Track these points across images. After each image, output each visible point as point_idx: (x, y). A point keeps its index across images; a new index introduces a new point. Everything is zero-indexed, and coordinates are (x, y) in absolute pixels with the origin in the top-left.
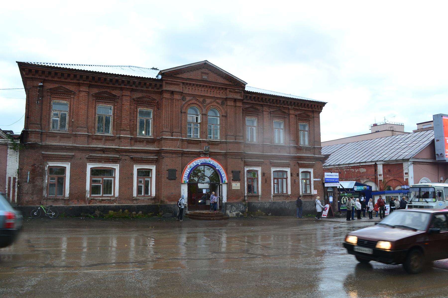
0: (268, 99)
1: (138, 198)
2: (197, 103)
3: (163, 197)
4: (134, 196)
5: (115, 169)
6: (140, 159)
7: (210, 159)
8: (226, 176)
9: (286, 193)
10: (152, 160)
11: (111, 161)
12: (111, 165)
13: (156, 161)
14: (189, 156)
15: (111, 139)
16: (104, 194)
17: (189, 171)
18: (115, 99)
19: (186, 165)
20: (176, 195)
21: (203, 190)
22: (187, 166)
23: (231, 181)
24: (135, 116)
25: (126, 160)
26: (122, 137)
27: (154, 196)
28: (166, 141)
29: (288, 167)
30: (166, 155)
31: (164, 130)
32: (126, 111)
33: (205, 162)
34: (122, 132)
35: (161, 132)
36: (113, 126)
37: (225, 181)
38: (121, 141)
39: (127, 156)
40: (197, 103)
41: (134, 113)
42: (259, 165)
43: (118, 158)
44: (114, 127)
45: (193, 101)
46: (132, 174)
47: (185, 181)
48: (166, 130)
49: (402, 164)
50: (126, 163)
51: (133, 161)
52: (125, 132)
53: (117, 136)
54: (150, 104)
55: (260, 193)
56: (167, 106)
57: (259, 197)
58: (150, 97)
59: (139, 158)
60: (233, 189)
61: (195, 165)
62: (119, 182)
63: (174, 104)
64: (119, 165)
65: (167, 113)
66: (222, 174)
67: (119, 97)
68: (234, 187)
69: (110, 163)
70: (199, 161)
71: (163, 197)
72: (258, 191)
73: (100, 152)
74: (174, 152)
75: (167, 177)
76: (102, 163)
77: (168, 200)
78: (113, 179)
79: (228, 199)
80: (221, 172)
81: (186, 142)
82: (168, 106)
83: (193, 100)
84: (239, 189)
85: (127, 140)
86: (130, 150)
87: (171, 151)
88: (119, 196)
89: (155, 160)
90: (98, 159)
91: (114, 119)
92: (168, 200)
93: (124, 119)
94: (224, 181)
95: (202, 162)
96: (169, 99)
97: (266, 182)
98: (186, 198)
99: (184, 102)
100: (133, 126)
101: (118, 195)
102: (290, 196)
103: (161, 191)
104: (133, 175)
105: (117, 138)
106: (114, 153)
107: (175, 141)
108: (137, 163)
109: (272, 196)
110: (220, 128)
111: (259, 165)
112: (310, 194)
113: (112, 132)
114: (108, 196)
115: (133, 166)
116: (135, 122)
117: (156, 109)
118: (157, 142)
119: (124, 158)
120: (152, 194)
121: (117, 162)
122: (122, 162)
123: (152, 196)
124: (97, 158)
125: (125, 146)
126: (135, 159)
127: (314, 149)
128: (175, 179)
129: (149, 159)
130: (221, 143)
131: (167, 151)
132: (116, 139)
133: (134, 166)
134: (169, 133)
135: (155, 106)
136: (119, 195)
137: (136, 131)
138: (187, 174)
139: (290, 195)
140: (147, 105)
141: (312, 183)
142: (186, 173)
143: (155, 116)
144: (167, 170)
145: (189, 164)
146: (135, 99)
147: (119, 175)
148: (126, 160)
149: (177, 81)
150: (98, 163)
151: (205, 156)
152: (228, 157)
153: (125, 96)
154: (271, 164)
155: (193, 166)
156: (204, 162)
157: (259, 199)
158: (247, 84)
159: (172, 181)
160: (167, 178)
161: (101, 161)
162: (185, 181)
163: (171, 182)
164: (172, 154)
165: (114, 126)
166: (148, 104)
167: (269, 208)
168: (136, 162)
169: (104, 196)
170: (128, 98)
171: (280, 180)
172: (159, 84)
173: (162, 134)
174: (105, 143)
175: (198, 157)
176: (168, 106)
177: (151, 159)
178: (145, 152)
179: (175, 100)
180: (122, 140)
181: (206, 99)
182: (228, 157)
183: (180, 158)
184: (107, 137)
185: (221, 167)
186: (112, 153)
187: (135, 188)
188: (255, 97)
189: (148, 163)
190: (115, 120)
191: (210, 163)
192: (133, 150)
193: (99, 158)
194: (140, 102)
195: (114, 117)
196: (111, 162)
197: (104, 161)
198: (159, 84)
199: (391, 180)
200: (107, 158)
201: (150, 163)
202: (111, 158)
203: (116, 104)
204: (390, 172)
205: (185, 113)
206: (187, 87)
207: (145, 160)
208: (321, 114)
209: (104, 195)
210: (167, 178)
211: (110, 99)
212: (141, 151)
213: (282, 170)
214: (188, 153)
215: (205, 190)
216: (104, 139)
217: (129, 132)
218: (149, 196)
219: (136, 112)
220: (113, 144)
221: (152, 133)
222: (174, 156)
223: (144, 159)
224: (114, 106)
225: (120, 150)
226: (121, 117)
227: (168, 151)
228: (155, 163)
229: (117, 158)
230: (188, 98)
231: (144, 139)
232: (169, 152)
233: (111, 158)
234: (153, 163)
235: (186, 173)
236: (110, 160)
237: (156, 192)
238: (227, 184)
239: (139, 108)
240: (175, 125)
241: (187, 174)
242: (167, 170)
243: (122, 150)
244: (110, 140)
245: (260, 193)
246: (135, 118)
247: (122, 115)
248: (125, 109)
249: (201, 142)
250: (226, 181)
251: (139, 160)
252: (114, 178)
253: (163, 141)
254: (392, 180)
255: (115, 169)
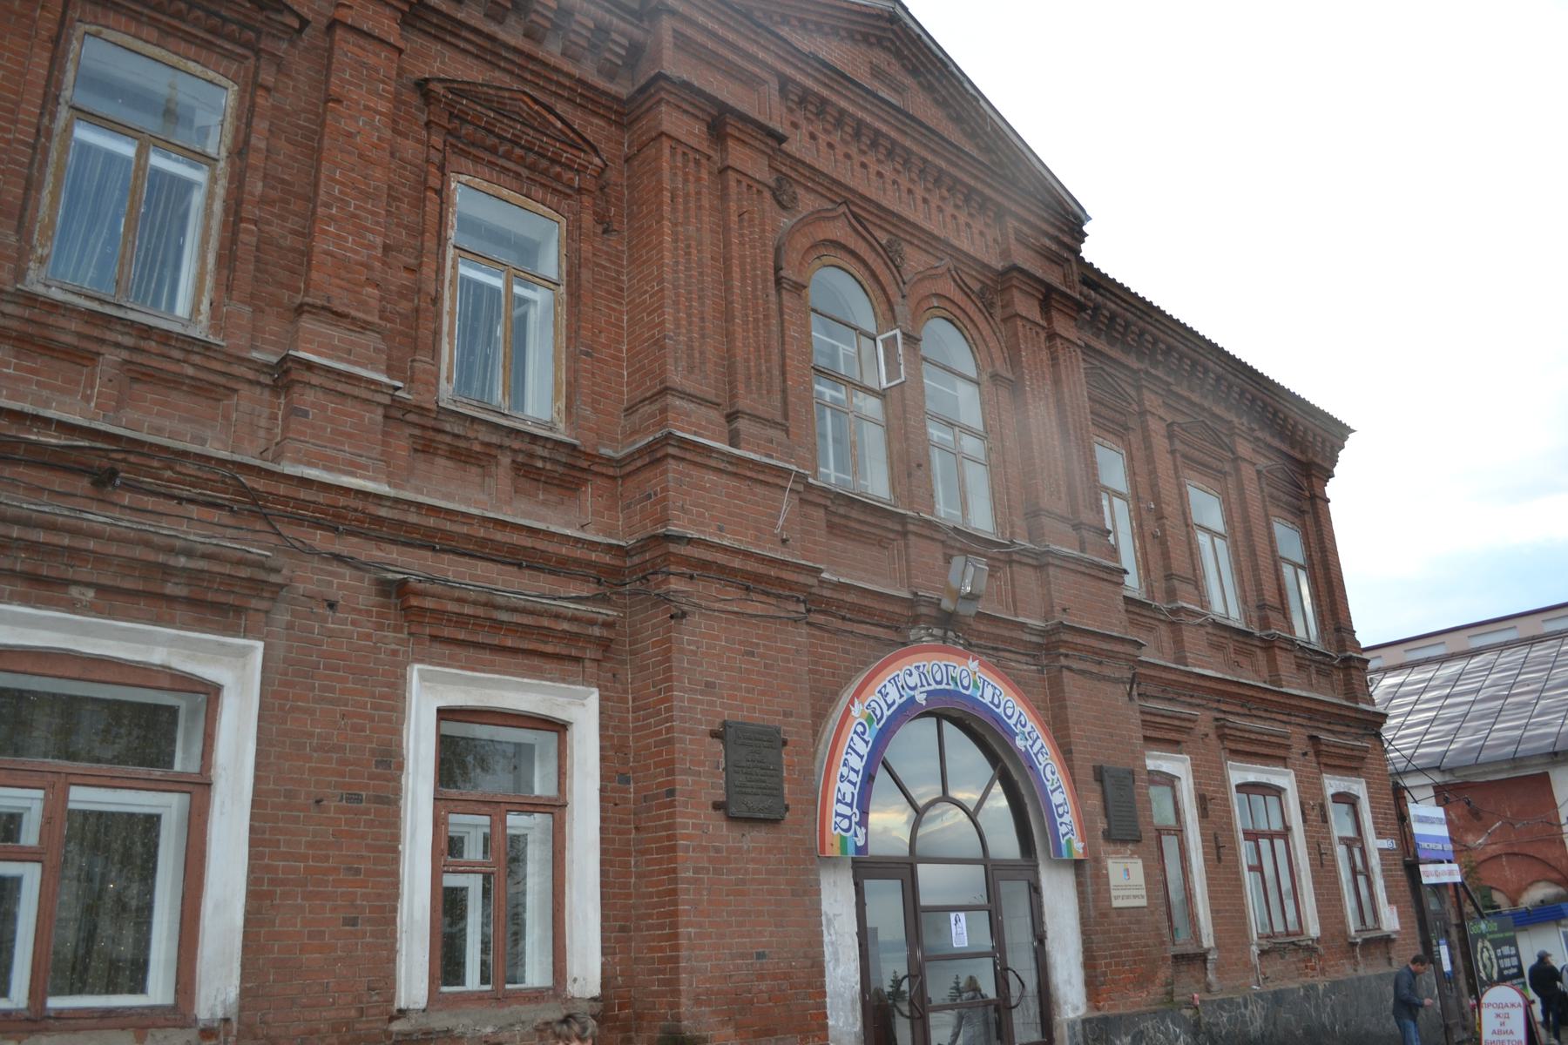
0: (1162, 346)
1: (440, 1021)
2: (862, 249)
3: (697, 1002)
4: (402, 1001)
5: (212, 692)
6: (467, 610)
7: (973, 665)
8: (1069, 807)
9: (1297, 928)
10: (574, 628)
11: (182, 591)
12: (171, 643)
13: (605, 645)
14: (848, 626)
15: (190, 371)
16: (59, 992)
17: (864, 749)
18: (259, 32)
19: (833, 698)
20: (787, 976)
21: (953, 916)
22: (847, 712)
23: (1103, 847)
24: (431, 220)
25: (332, 605)
26: (310, 366)
27: (594, 989)
28: (695, 472)
29: (1283, 761)
30: (699, 587)
31: (676, 378)
32: (361, 156)
33: (952, 687)
34: (307, 323)
35: (630, 410)
36: (220, 259)
37: (1069, 841)
38: (294, 412)
39: (347, 572)
40: (862, 249)
41: (419, 204)
42: (1177, 743)
43: (262, 575)
44: (233, 270)
45: (839, 230)
46: (390, 761)
47: (843, 839)
48: (690, 386)
49: (1543, 781)
50: (331, 634)
51: (398, 629)
52: (337, 334)
53: (255, 355)
54: (544, 172)
55: (1208, 941)
56: (686, 202)
57: (1205, 960)
58: (551, 118)
59: (461, 600)
60: (1116, 903)
61: (899, 701)
62: (253, 843)
63: (733, 206)
64: (260, 645)
65: (688, 254)
66: (1050, 788)
67: (304, 23)
68: (1118, 887)
69: (158, 621)
70: (915, 673)
71: (697, 1002)
72: (1192, 919)
73: (58, 481)
74: (758, 578)
75: (720, 795)
76: (72, 606)
77: (738, 1028)
78: (170, 807)
79: (1093, 986)
80: (1041, 768)
81: (822, 512)
82: (692, 205)
83: (838, 223)
84: (1143, 902)
85: (350, 406)
86: (383, 512)
87: (737, 563)
88: (242, 1008)
89: (597, 631)
90: (32, 546)
91: (239, 203)
92: (730, 1031)
93: (332, 218)
94: (1063, 842)
95: (934, 686)
96: (697, 162)
97: (1219, 859)
98: (853, 1002)
99: (786, 221)
100: (404, 306)
101: (233, 992)
102: (1320, 948)
103: (675, 936)
104: (401, 767)
105: (251, 375)
106: (216, 516)
107: (759, 489)
108: (437, 648)
109: (1255, 949)
110: (988, 456)
111: (1177, 743)
112: (1378, 934)
113: (205, 307)
114: (107, 1014)
115: (404, 676)
116: (428, 271)
117: (587, 219)
118: (599, 481)
119: (309, 578)
120: (574, 967)
121: (239, 610)
122: (290, 626)
123: (573, 990)
124: (15, 532)
125: (330, 464)
126: (429, 603)
127: (1349, 668)
128: (774, 822)
129: (546, 622)
130: (1011, 562)
131: (708, 555)
132: (245, 390)
133: (415, 671)
134: (714, 415)
135: (580, 191)
136: (244, 993)
137: (435, 352)
138: (853, 777)
139: (1318, 940)
140: (525, 172)
141: (1375, 861)
142: (845, 771)
143: (586, 275)
144: (714, 734)
145: (858, 693)
146: (439, 88)
147: (258, 766)
148: (332, 605)
149: (753, 49)
150: (25, 600)
151: (944, 639)
152: (1063, 661)
153: (351, 38)
154: (1222, 737)
155: (887, 713)
156: (943, 686)
157: (1211, 977)
158: (1089, 219)
159: (756, 838)
160: (717, 806)
161: (67, 583)
162: (843, 839)
163: (746, 844)
164: (741, 594)
165: (228, 258)
166: (532, 168)
167: (1263, 1036)
168: (434, 638)
169: (60, 1015)
170: (380, 59)
171: (1264, 844)
172: (623, 34)
173: (664, 410)
174: (120, 405)
175: (893, 644)
176: (692, 205)
177: (565, 626)
178: (514, 549)
179: (739, 182)
180: (310, 396)
181: (907, 249)
182: (1063, 661)
183: (802, 635)
184: (152, 345)
185: (1038, 732)
186: (194, 511)
187: (411, 915)
188: (1113, 317)
189: (536, 662)
190: (249, 210)
191: (978, 695)
192: (413, 518)
193: (41, 536)
194: (467, 130)
195: (237, 181)
196: (180, 612)
197: (101, 589)
198: (623, 34)
199: (1492, 858)
200: (139, 552)
201: (548, 665)
202: (182, 561)
203: (267, 77)
204: (1480, 819)
205: (799, 288)
206: (803, 123)
207: (513, 628)
208: (1332, 489)
209: (55, 1003)
210: (717, 806)
211: (215, 21)
212: (484, 542)
213: (1263, 778)
214: (841, 604)
215: (962, 915)
216: (111, 356)
217: (372, 340)
218: (537, 996)
219: (439, 192)
220: (209, 433)
221: (562, 404)
222: (756, 606)
223: (504, 616)
224: (251, 88)
225: (282, 489)
226: (312, 199)
227: (721, 558)
228: (590, 667)
229: (244, 572)
230: (808, 203)
231: (495, 439)
232: (722, 569)
233: (182, 561)
234: (577, 660)
235: (845, 771)
236: (170, 589)
237: (605, 952)
238: (1078, 865)
239: (464, 178)
240: (747, 360)
241: (853, 777)
242: (716, 727)
243: (303, 494)
244: (173, 382)
245: (1208, 941)
246: (430, 244)
247: (316, 185)
248: (350, 135)
249: (905, 534)
250: (1078, 847)
251: (461, 621)
252: (199, 788)
253: (672, 464)
254: (1499, 856)
255: (212, 692)
